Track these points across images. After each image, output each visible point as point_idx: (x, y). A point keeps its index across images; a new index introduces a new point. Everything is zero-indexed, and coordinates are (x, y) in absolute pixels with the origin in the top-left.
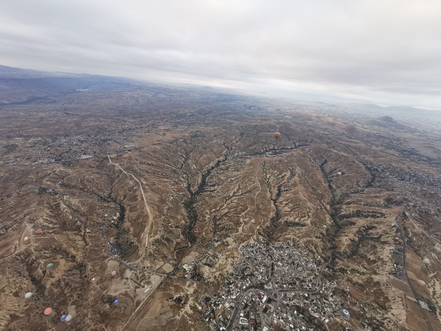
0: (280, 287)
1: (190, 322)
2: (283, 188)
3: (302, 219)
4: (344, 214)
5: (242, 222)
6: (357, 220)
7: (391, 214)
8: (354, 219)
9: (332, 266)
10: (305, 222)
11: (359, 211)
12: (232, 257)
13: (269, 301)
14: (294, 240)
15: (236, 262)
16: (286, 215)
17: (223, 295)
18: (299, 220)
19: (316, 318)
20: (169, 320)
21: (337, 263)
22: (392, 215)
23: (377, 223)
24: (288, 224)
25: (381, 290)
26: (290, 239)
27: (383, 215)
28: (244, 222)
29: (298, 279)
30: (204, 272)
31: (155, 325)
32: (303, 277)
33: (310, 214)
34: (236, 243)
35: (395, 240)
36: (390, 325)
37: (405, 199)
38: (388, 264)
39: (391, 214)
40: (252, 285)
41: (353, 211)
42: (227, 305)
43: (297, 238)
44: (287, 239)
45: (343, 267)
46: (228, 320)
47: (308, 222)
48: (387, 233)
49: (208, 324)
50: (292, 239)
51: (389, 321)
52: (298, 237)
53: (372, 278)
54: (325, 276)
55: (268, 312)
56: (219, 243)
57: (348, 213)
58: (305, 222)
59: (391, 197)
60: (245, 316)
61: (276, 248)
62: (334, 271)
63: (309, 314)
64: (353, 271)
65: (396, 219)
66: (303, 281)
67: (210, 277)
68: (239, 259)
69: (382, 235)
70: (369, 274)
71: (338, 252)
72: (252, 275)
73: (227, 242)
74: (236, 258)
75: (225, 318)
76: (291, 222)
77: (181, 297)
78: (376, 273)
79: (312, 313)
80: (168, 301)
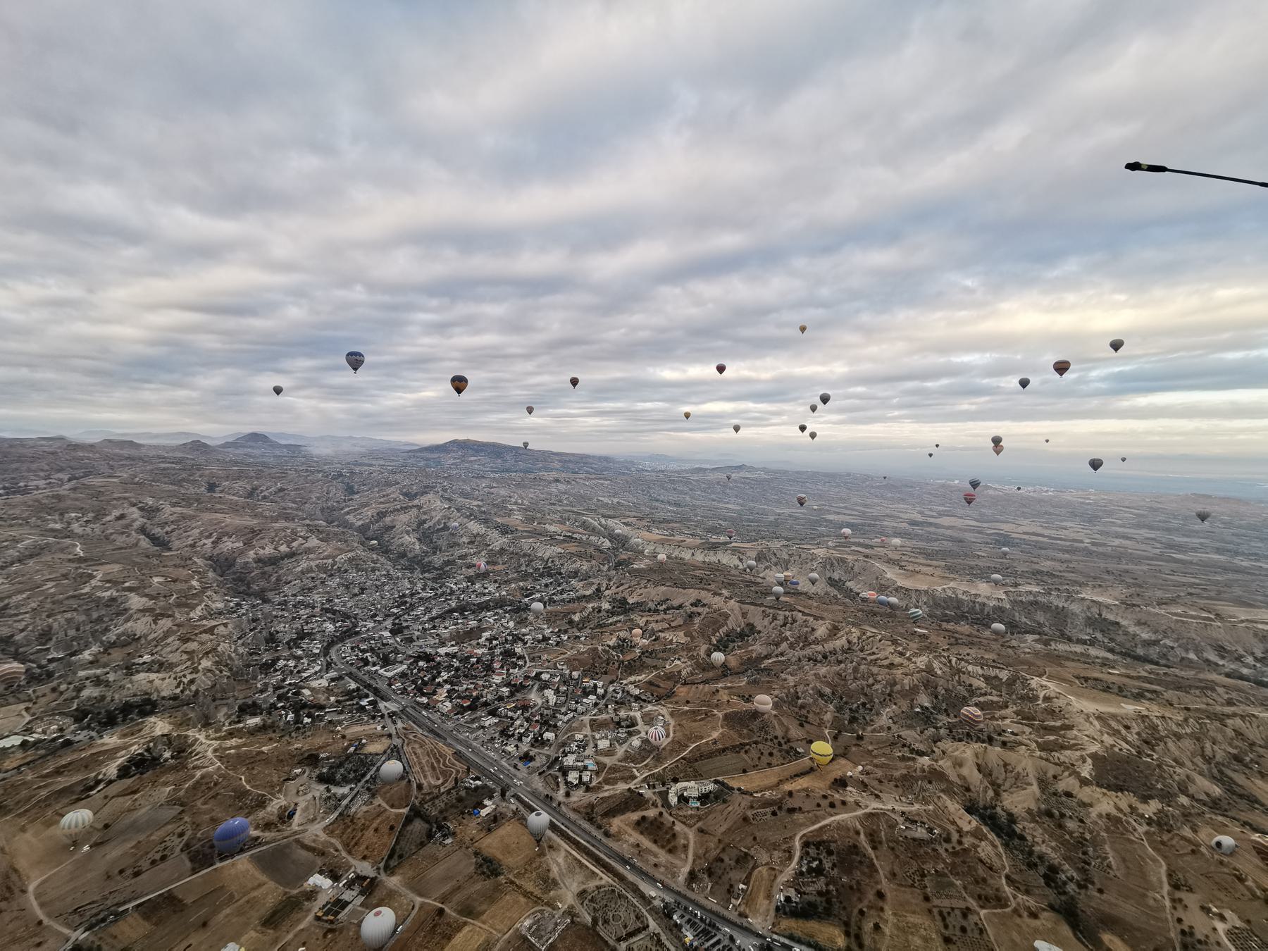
0: (388, 616)
1: (265, 749)
2: (157, 531)
3: (295, 544)
4: (362, 525)
5: (115, 594)
6: (392, 521)
7: (429, 501)
8: (388, 520)
9: (426, 568)
10: (306, 545)
11: (382, 513)
12: (205, 632)
13: (395, 632)
14: (323, 568)
15: (229, 636)
16: (242, 553)
17: (284, 680)
18: (288, 547)
19: (489, 600)
20: (182, 793)
21: (430, 562)
22: (432, 501)
23: (425, 513)
24: (274, 561)
25: (513, 553)
26: (310, 570)
27: (419, 507)
28: (130, 589)
29: (404, 596)
30: (145, 687)
31: (133, 843)
32: (409, 589)
33: (302, 534)
34: (169, 616)
35: (467, 517)
36: (557, 563)
37: (425, 487)
38: (489, 533)
39: (429, 501)
40: (325, 644)
41: (373, 516)
42: (324, 683)
43: (325, 561)
44: (302, 572)
45: (446, 559)
46: (358, 689)
47: (313, 542)
48: (449, 518)
49: (321, 720)
50: (314, 567)
51: (552, 561)
52: (327, 558)
53: (492, 550)
54: (435, 580)
55: (415, 638)
56: (95, 649)
57: (367, 521)
58: (306, 545)
59: (404, 490)
60: (381, 668)
61: (293, 595)
62: (442, 569)
63: (474, 605)
64: (460, 558)
65: (442, 502)
66: (412, 595)
67: (192, 681)
68: (230, 626)
69: (445, 523)
70: (483, 550)
71: (414, 557)
72: (302, 635)
73: (119, 636)
74: (222, 628)
75: (350, 694)
76: (270, 559)
77: (141, 754)
78: (489, 545)
79: (479, 600)
80: (88, 796)
